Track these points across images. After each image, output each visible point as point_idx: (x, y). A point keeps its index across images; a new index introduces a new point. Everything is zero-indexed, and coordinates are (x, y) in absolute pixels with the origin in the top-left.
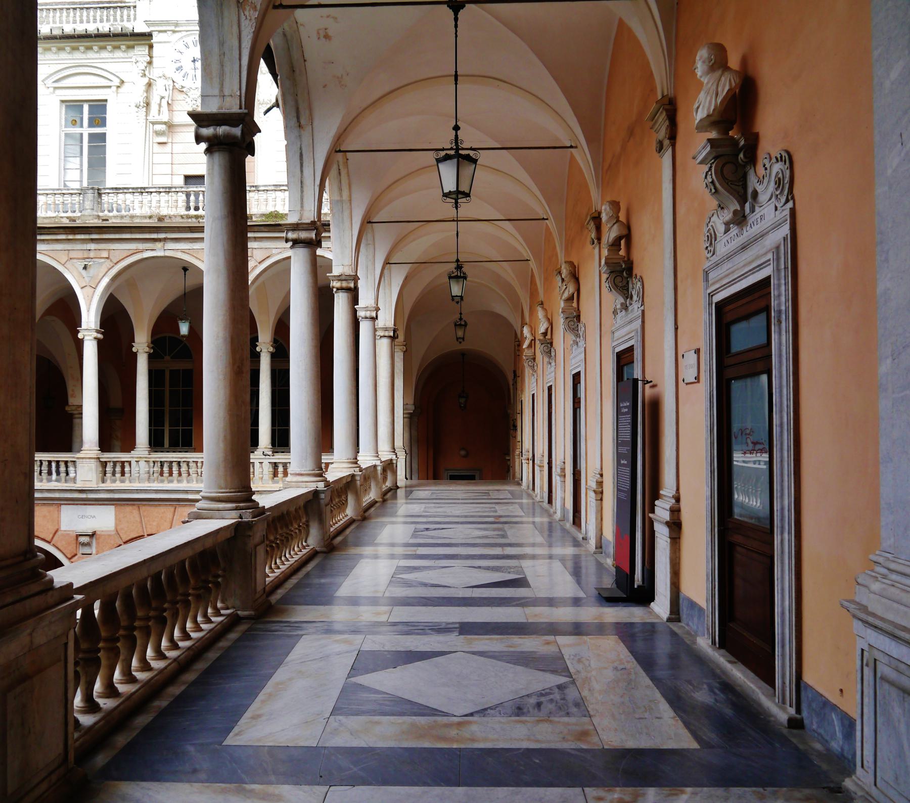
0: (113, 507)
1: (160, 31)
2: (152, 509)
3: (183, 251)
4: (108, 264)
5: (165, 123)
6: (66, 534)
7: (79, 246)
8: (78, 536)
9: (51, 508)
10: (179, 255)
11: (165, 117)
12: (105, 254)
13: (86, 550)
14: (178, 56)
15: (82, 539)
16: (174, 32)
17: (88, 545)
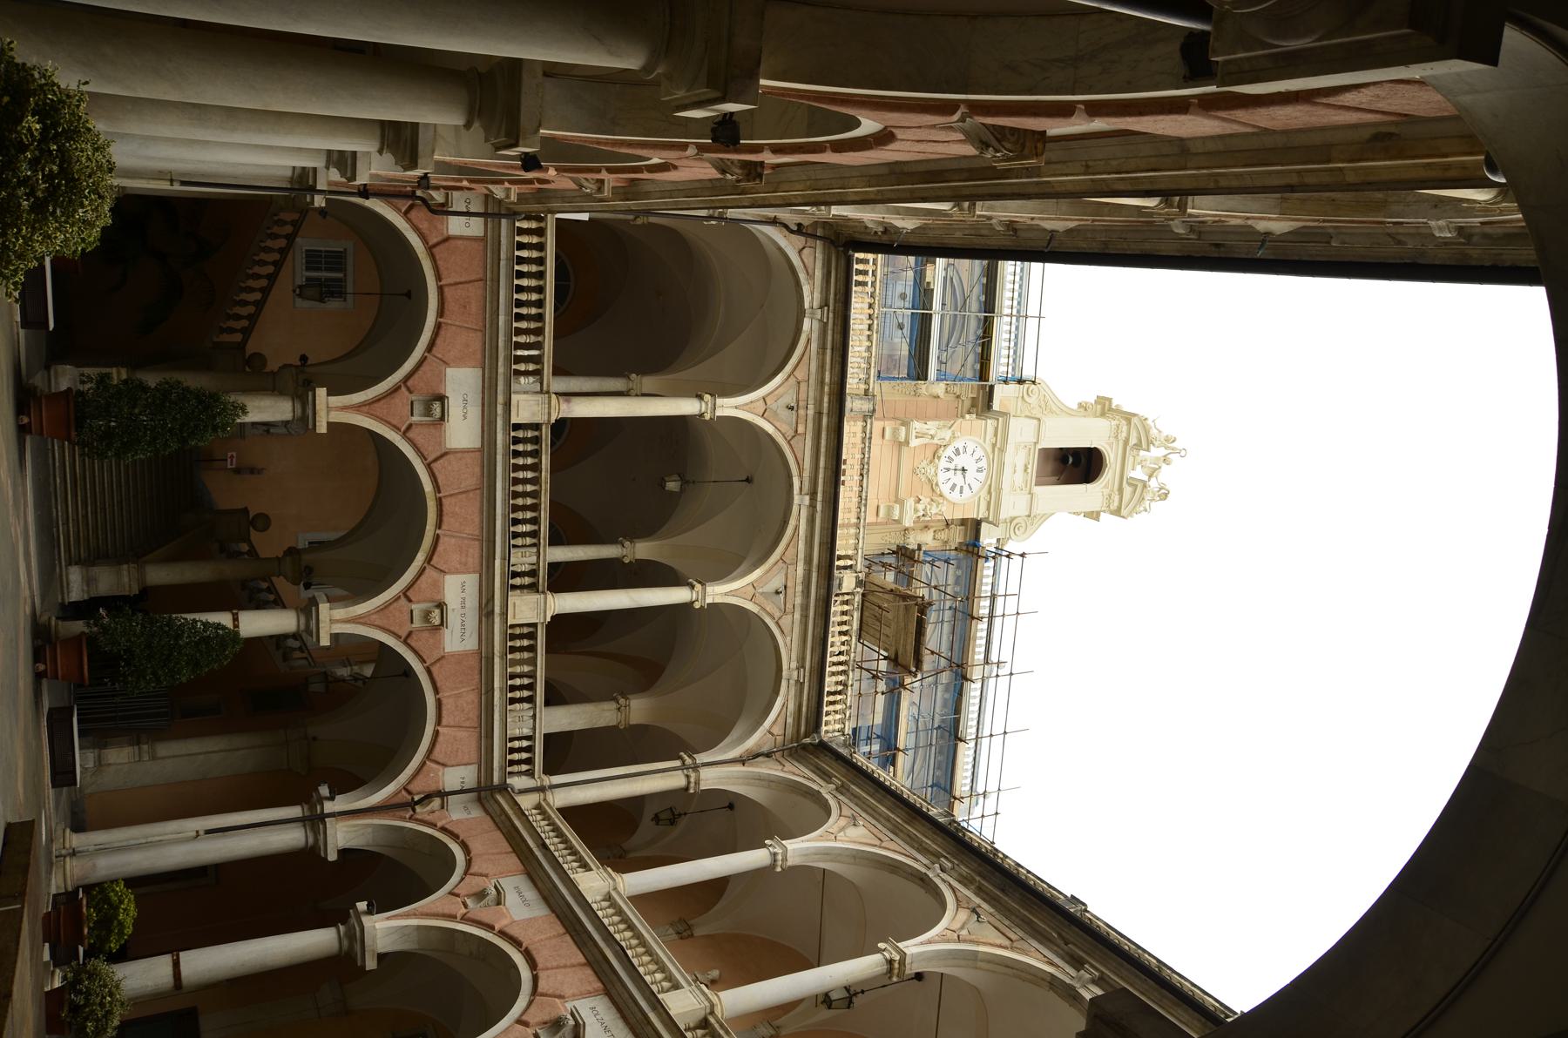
0: (478, 445)
1: (996, 429)
2: (478, 504)
3: (797, 528)
4: (790, 433)
5: (907, 442)
6: (441, 379)
7: (811, 394)
8: (441, 399)
9: (479, 356)
10: (792, 522)
11: (914, 443)
12: (801, 429)
13: (418, 408)
14: (970, 451)
15: (437, 406)
16: (994, 445)
17: (428, 411)
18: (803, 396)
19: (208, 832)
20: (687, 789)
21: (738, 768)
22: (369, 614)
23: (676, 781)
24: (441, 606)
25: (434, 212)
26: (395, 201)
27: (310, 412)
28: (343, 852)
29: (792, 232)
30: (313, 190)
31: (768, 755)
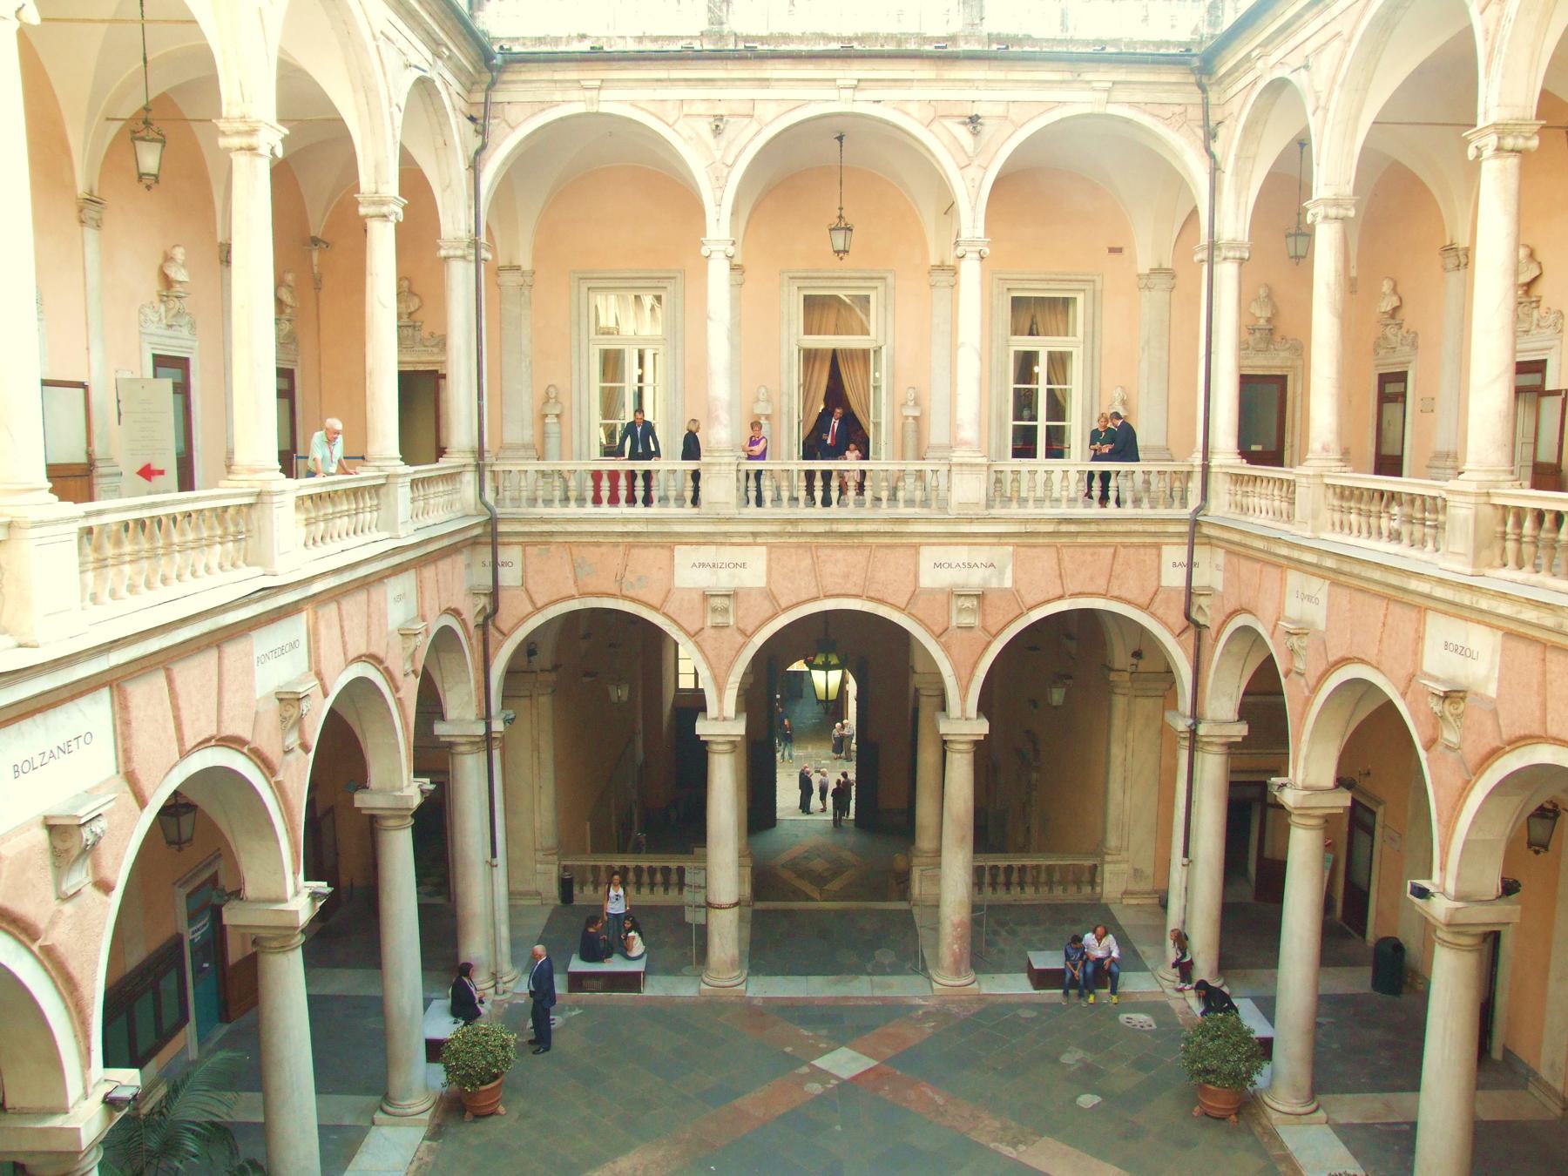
8: (706, 596)
15: (717, 602)
18: (700, 108)
19: (1186, 853)
20: (1241, 261)
21: (1227, 180)
22: (958, 678)
23: (1227, 273)
24: (954, 594)
25: (495, 610)
26: (491, 650)
27: (720, 739)
28: (1244, 712)
29: (484, 147)
30: (488, 737)
31: (1210, 136)
